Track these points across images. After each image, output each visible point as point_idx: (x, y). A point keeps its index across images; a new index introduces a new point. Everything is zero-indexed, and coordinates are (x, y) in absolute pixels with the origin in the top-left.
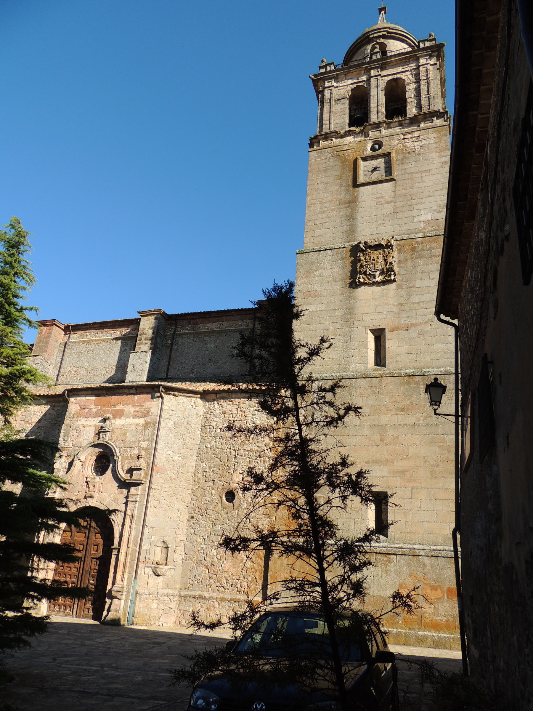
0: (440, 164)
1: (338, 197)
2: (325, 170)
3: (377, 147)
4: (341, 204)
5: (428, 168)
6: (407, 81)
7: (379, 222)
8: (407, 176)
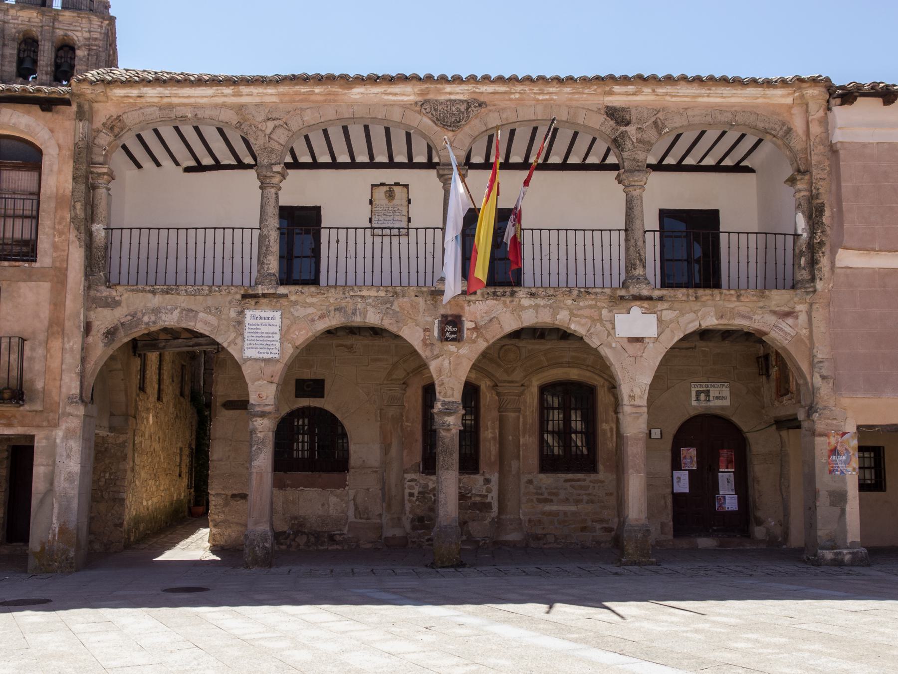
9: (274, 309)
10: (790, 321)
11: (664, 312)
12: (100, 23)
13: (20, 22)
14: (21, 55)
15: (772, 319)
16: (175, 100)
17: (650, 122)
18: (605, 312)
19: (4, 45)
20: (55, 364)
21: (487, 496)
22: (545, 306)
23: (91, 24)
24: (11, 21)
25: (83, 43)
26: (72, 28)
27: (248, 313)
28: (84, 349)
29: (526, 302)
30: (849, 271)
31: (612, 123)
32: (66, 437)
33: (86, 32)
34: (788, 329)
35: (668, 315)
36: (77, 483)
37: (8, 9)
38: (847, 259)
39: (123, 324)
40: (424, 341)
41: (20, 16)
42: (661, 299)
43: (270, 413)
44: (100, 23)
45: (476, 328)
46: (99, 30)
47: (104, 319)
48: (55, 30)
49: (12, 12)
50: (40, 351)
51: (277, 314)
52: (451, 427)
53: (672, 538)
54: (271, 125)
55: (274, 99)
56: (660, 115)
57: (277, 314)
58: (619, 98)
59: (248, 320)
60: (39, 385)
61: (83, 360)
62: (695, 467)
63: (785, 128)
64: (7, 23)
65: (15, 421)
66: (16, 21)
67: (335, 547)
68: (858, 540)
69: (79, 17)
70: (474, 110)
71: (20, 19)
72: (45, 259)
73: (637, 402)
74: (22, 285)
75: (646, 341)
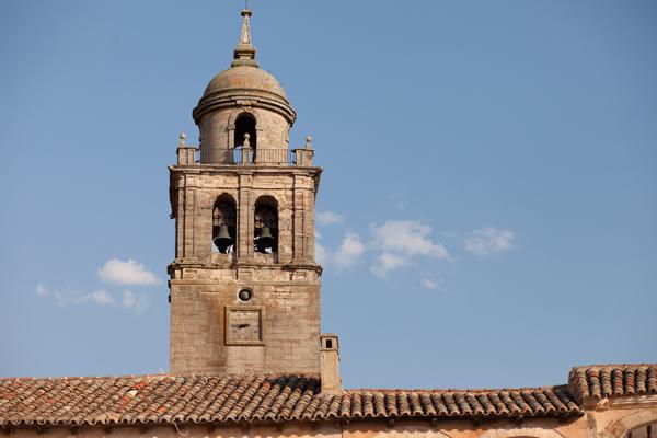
1: (205, 355)
2: (190, 315)
3: (246, 294)
4: (208, 365)
6: (281, 205)
14: (216, 224)
24: (205, 185)
66: (209, 185)
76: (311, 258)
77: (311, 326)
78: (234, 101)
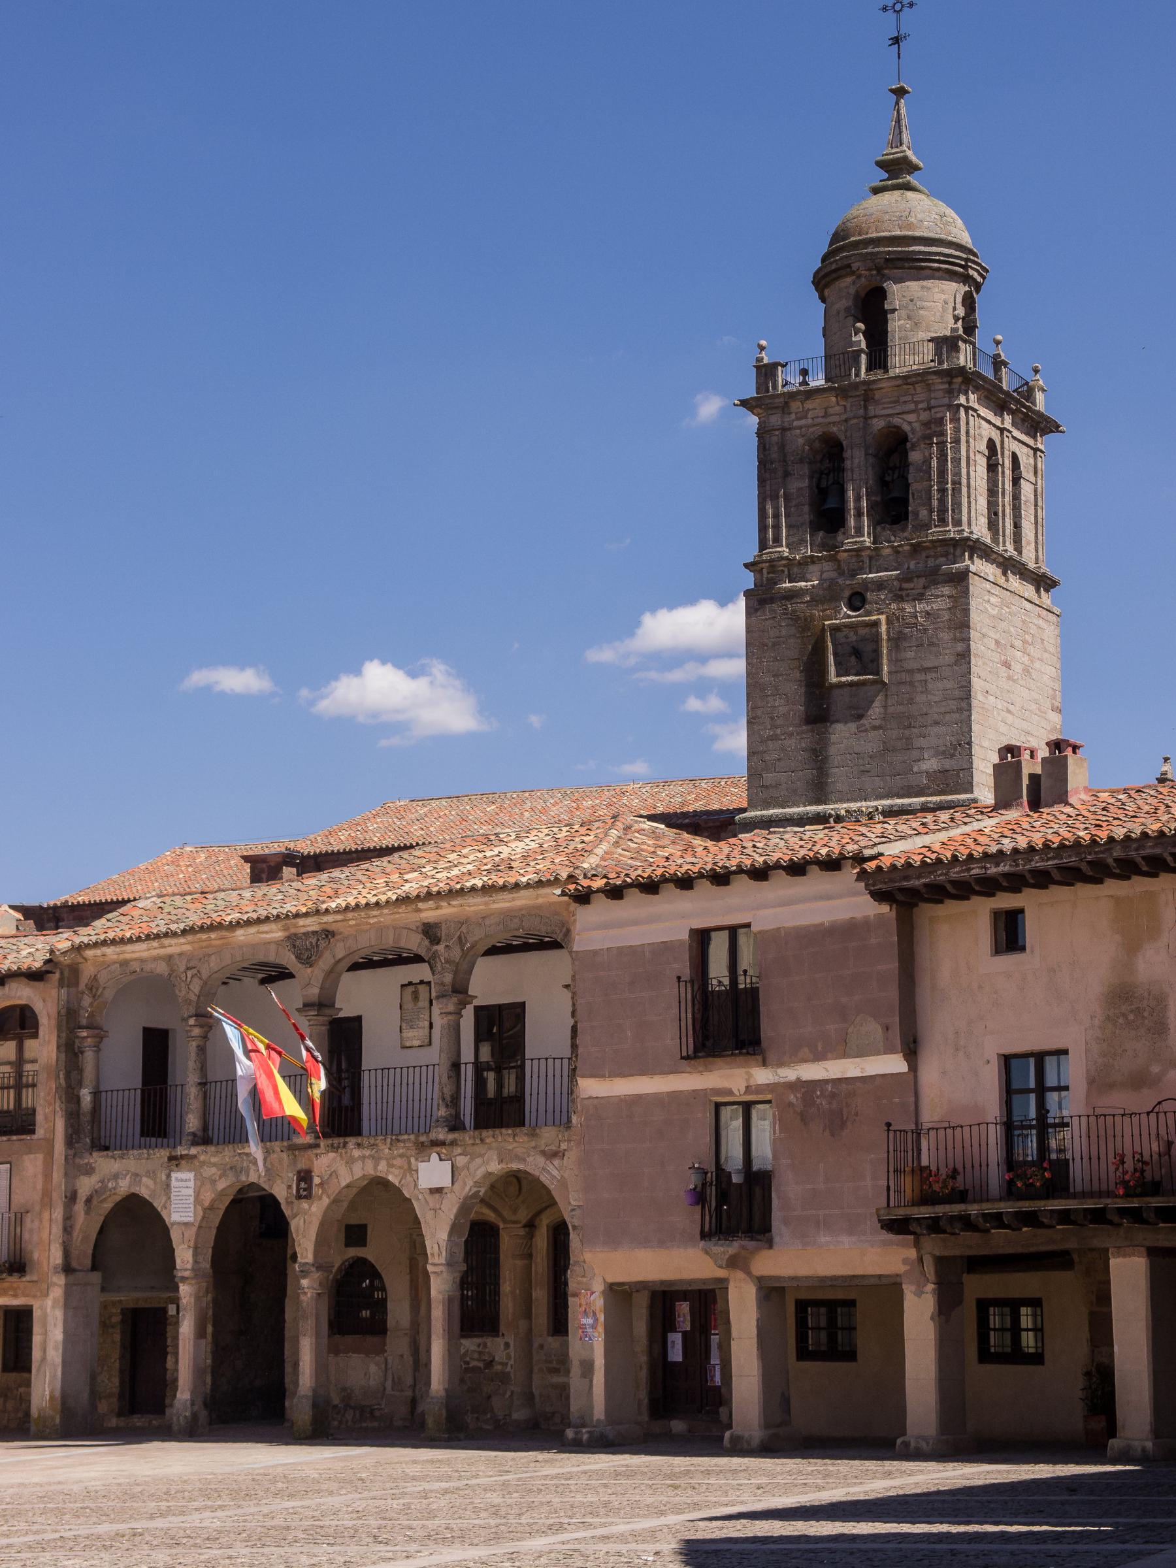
0: (953, 659)
5: (936, 664)
7: (862, 768)
8: (903, 675)
9: (190, 1171)
10: (556, 1162)
11: (458, 1158)
12: (946, 386)
13: (810, 421)
14: (824, 484)
15: (541, 1160)
16: (128, 956)
17: (456, 937)
18: (413, 1160)
19: (787, 474)
20: (45, 1235)
21: (506, 1364)
22: (368, 1157)
23: (930, 390)
24: (796, 423)
25: (920, 434)
26: (899, 409)
27: (174, 1175)
28: (68, 1218)
29: (357, 1153)
30: (596, 1101)
31: (427, 942)
32: (53, 1307)
33: (925, 410)
34: (555, 1173)
35: (461, 1161)
36: (61, 1351)
37: (786, 403)
38: (590, 1087)
39: (96, 1191)
40: (286, 1199)
41: (809, 410)
42: (453, 1143)
43: (187, 1278)
44: (946, 386)
45: (321, 1185)
46: (946, 401)
47: (85, 1185)
48: (869, 422)
49: (795, 406)
50: (37, 1223)
51: (191, 1175)
52: (306, 1290)
53: (646, 1419)
54: (189, 974)
55: (188, 948)
56: (464, 929)
57: (191, 1175)
58: (429, 913)
59: (174, 1183)
60: (36, 1256)
61: (67, 1230)
62: (688, 1329)
63: (564, 929)
64: (789, 429)
65: (19, 1292)
66: (803, 422)
67: (376, 1424)
68: (603, 1418)
69: (907, 384)
70: (322, 944)
71: (810, 415)
72: (40, 1132)
73: (436, 1261)
74: (26, 1157)
75: (445, 1191)
76: (958, 523)
77: (955, 639)
78: (849, 266)
